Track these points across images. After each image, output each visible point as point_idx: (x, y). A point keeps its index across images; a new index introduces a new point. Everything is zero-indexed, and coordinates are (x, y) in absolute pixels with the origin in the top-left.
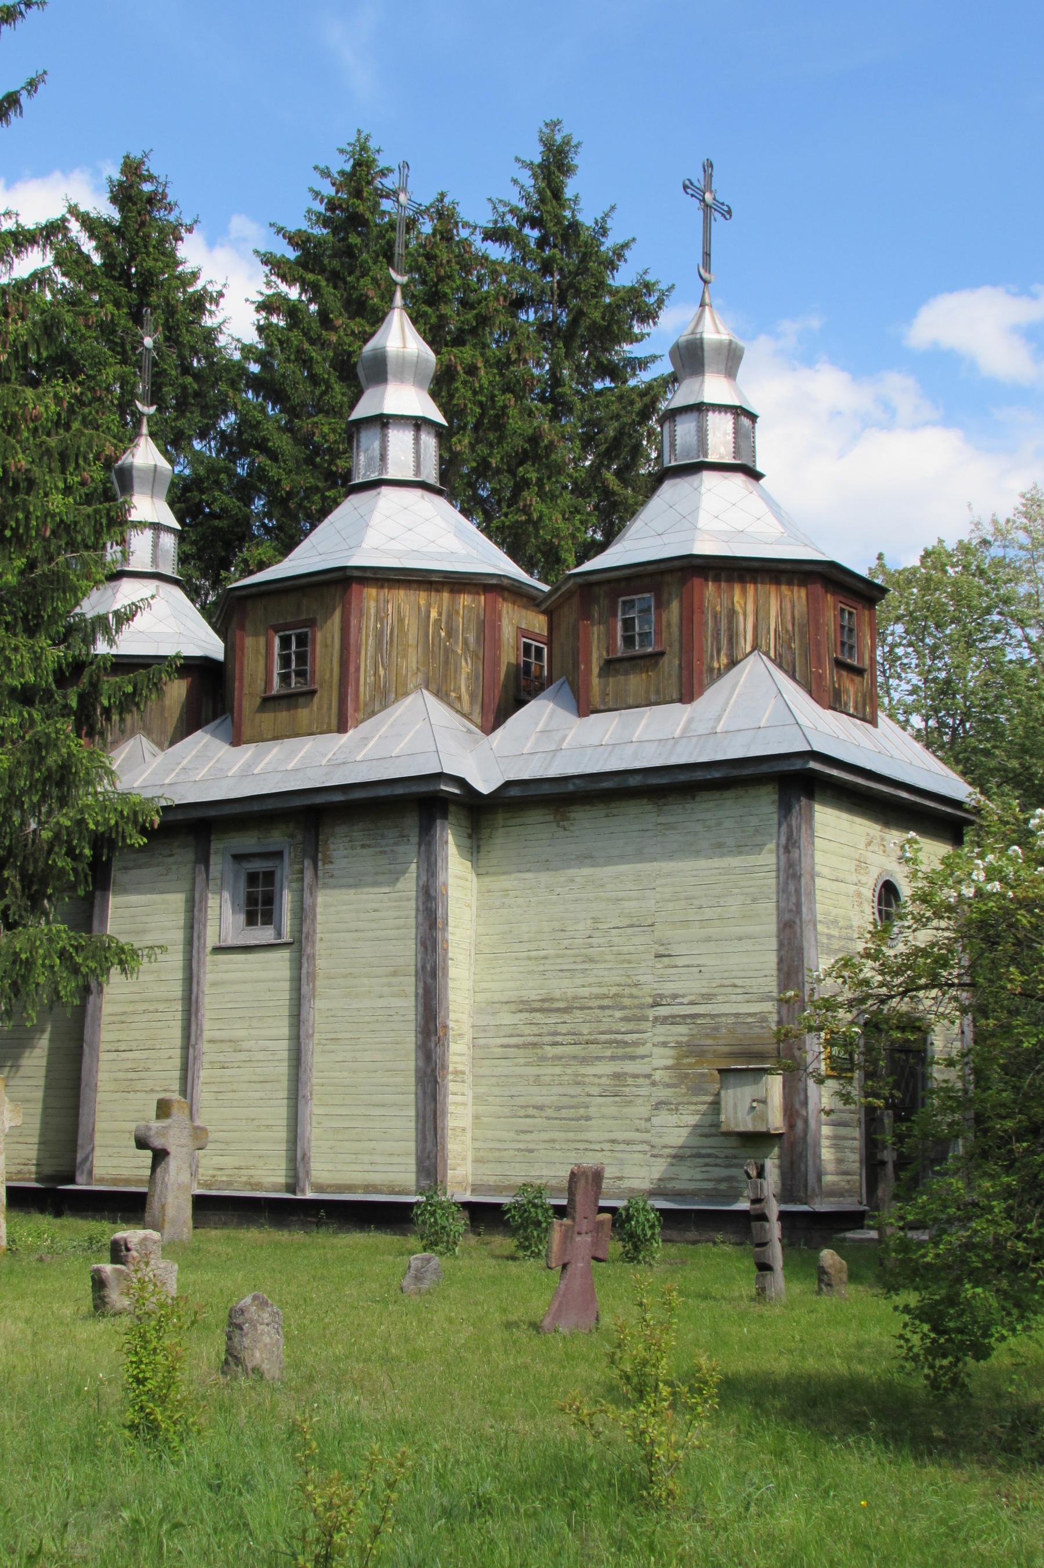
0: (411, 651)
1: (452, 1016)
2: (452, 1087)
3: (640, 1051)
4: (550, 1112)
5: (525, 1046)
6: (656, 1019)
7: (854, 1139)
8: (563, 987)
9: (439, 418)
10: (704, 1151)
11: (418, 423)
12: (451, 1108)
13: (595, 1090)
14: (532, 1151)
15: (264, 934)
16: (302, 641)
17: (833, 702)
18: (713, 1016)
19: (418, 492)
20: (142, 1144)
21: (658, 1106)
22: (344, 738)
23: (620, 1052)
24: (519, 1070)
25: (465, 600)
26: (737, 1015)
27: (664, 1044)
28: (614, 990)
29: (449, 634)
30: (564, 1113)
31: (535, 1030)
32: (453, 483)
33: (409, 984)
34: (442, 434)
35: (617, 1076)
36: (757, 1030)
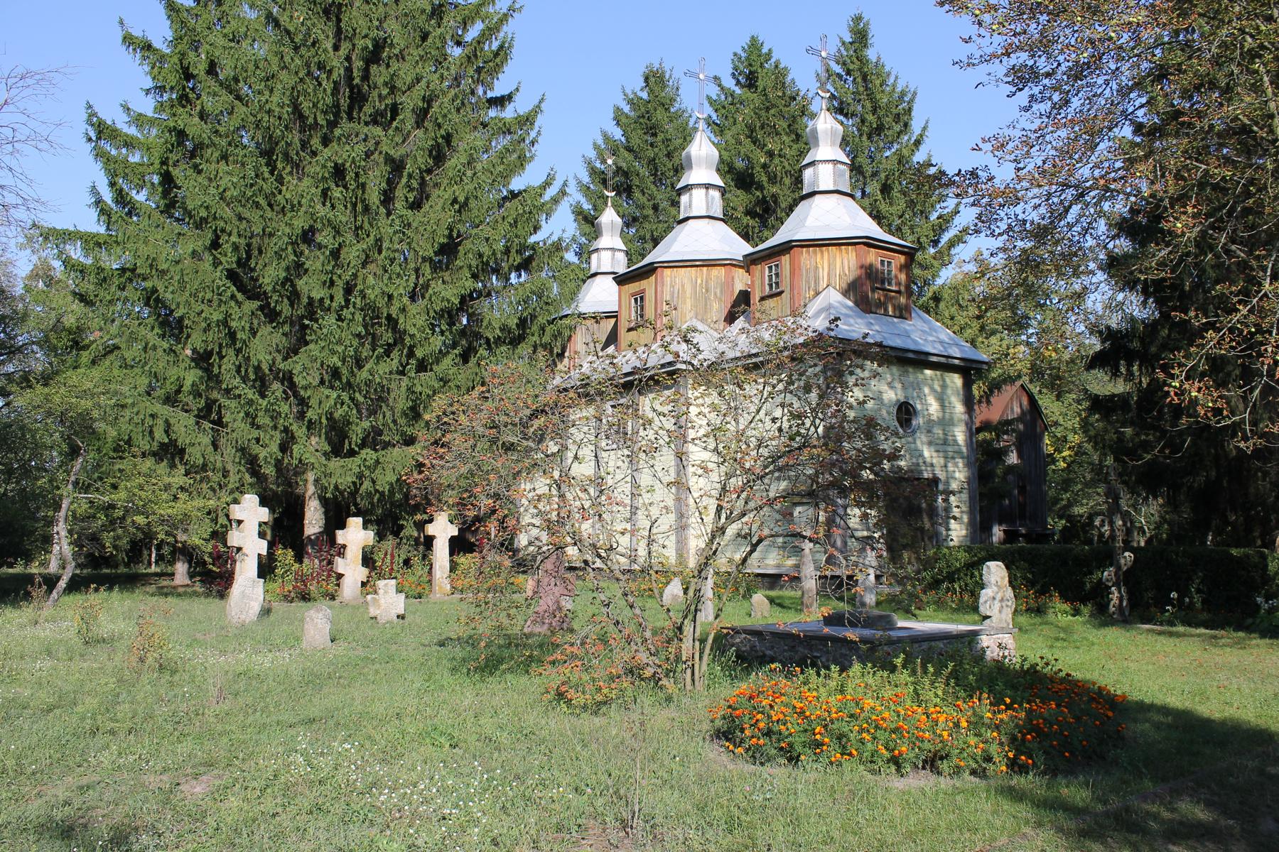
0: (688, 301)
11: (708, 186)
16: (642, 298)
19: (707, 220)
25: (716, 272)
29: (707, 291)
34: (723, 192)
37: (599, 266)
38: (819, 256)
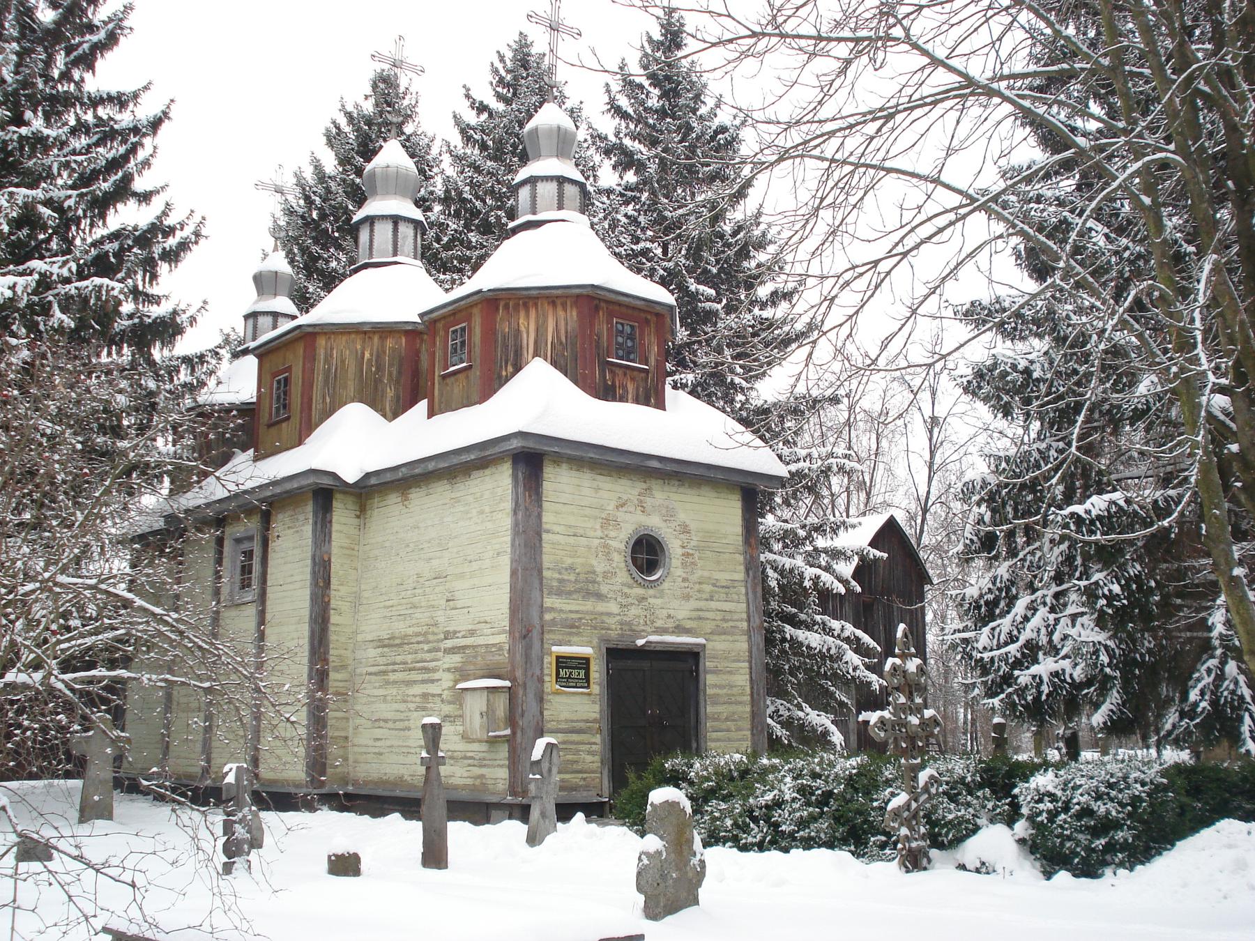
1: (331, 652)
3: (436, 676)
7: (595, 743)
8: (400, 627)
10: (469, 754)
11: (396, 220)
14: (381, 754)
17: (606, 392)
23: (426, 676)
25: (389, 343)
27: (449, 670)
30: (390, 725)
33: (305, 630)
35: (425, 696)
36: (497, 657)
38: (522, 314)
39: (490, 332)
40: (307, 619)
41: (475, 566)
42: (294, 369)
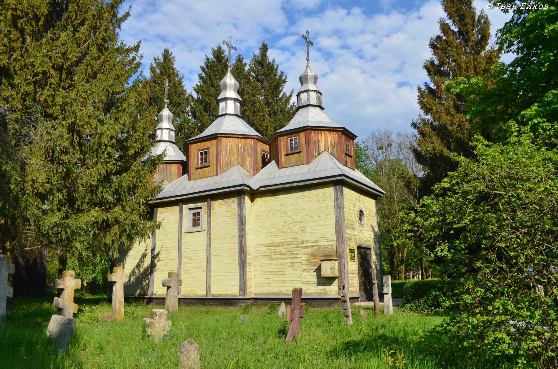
2: (248, 267)
3: (298, 256)
4: (274, 273)
5: (267, 256)
6: (302, 247)
8: (277, 240)
9: (240, 98)
12: (248, 273)
13: (286, 267)
15: (196, 229)
16: (206, 153)
18: (318, 246)
19: (235, 117)
20: (164, 285)
21: (304, 270)
22: (217, 177)
23: (293, 256)
24: (266, 262)
25: (248, 141)
26: (324, 245)
27: (305, 254)
28: (291, 240)
29: (244, 151)
30: (278, 273)
31: (270, 251)
32: (243, 116)
33: (236, 241)
35: (292, 263)
37: (161, 137)
39: (308, 141)
40: (237, 237)
41: (316, 218)
42: (211, 149)
